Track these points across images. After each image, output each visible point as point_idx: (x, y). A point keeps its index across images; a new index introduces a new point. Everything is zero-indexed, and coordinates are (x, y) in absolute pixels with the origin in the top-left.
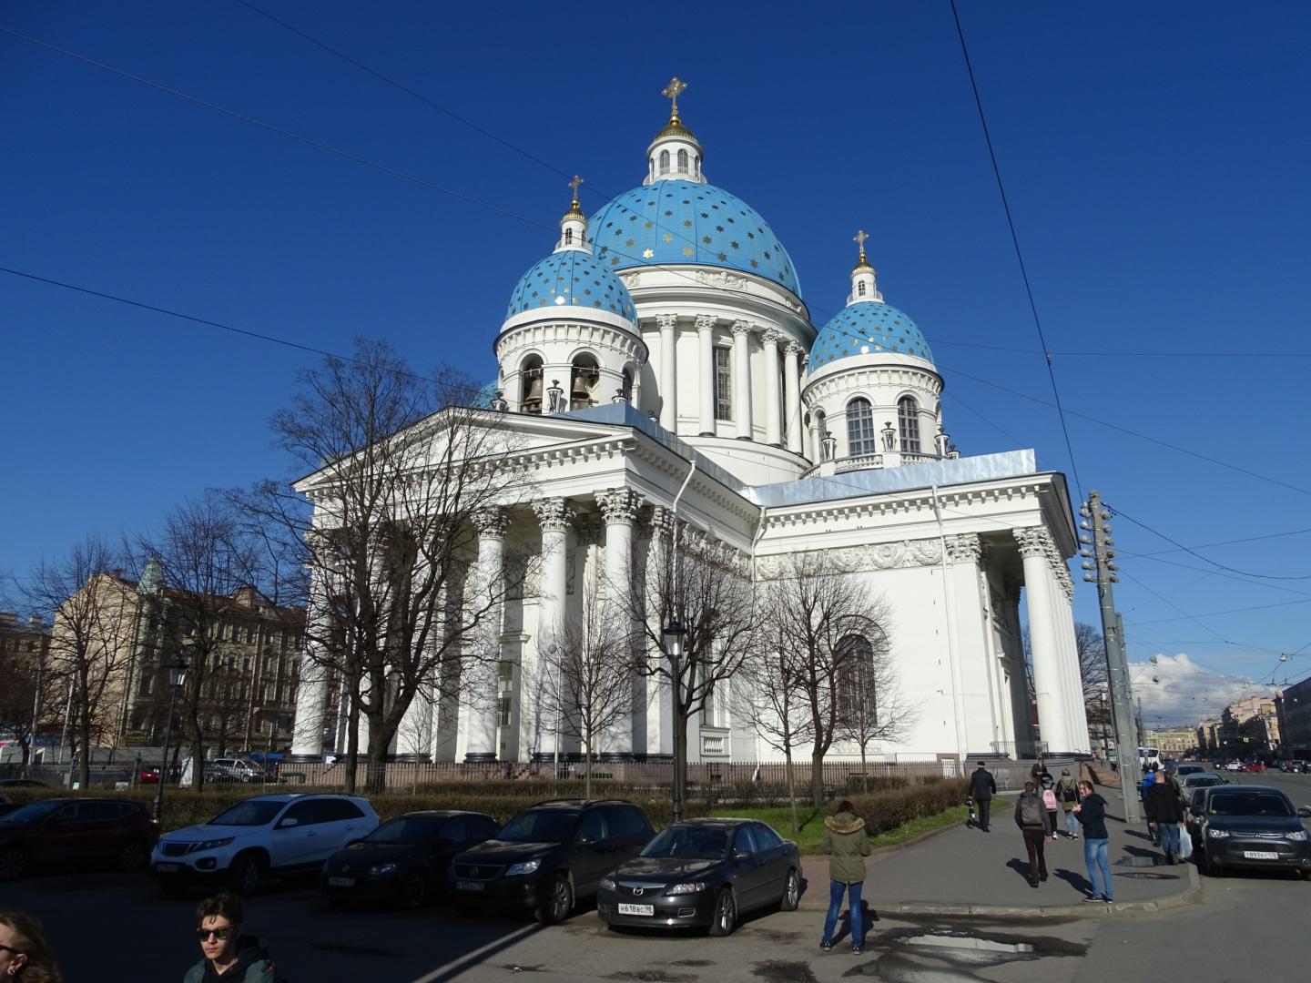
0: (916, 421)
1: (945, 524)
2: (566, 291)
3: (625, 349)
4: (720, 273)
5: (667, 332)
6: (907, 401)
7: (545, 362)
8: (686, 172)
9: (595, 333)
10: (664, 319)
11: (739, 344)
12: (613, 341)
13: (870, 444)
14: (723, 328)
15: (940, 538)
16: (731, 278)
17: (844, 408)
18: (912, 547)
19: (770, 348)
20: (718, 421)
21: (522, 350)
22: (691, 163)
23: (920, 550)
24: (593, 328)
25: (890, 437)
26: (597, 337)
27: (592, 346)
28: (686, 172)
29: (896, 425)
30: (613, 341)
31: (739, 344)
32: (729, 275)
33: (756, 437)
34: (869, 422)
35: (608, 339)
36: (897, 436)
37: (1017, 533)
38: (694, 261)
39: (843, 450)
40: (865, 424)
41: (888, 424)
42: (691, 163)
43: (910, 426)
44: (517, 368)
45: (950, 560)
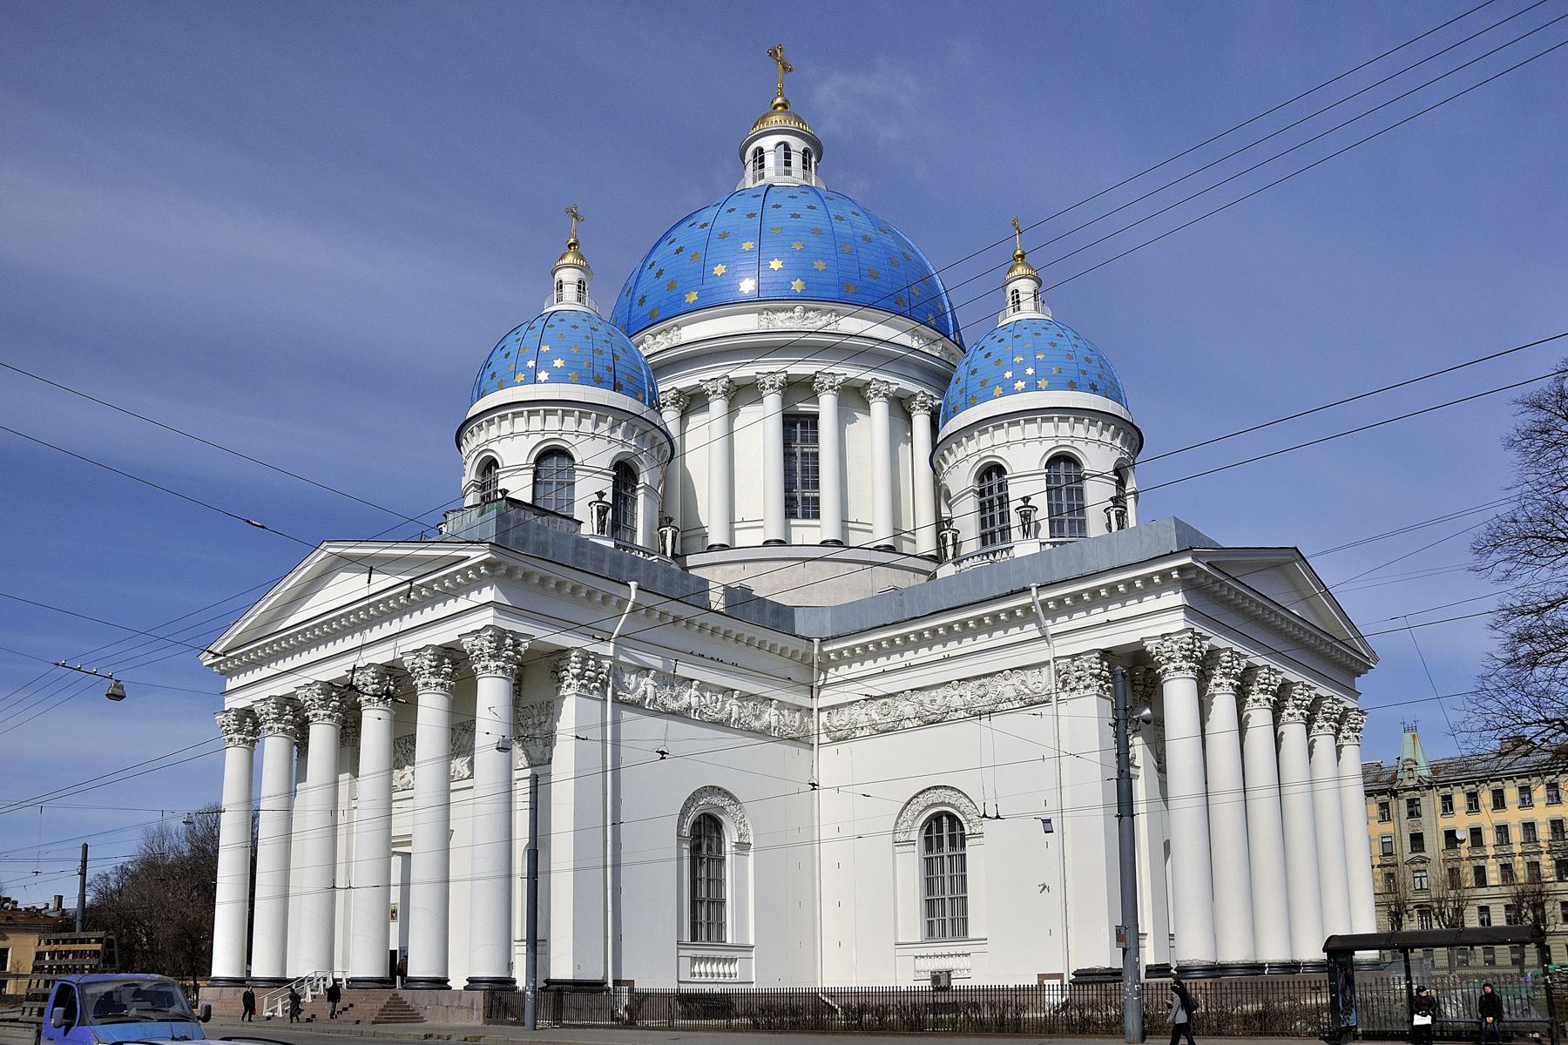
0: (1080, 491)
1: (1057, 642)
2: (531, 364)
4: (792, 310)
5: (718, 406)
6: (1062, 464)
7: (500, 466)
8: (788, 173)
10: (710, 386)
11: (826, 406)
12: (596, 426)
13: (1005, 532)
14: (797, 388)
15: (1047, 663)
16: (811, 314)
17: (970, 483)
18: (1015, 680)
19: (879, 408)
20: (793, 522)
21: (476, 453)
22: (796, 160)
23: (1023, 682)
25: (1026, 518)
26: (570, 423)
27: (563, 437)
28: (788, 173)
29: (1041, 502)
30: (596, 426)
31: (826, 406)
32: (806, 310)
33: (855, 539)
34: (1004, 501)
36: (1042, 514)
37: (1150, 646)
38: (777, 295)
39: (971, 545)
40: (1001, 505)
41: (1026, 499)
42: (796, 160)
43: (1069, 497)
45: (1063, 695)
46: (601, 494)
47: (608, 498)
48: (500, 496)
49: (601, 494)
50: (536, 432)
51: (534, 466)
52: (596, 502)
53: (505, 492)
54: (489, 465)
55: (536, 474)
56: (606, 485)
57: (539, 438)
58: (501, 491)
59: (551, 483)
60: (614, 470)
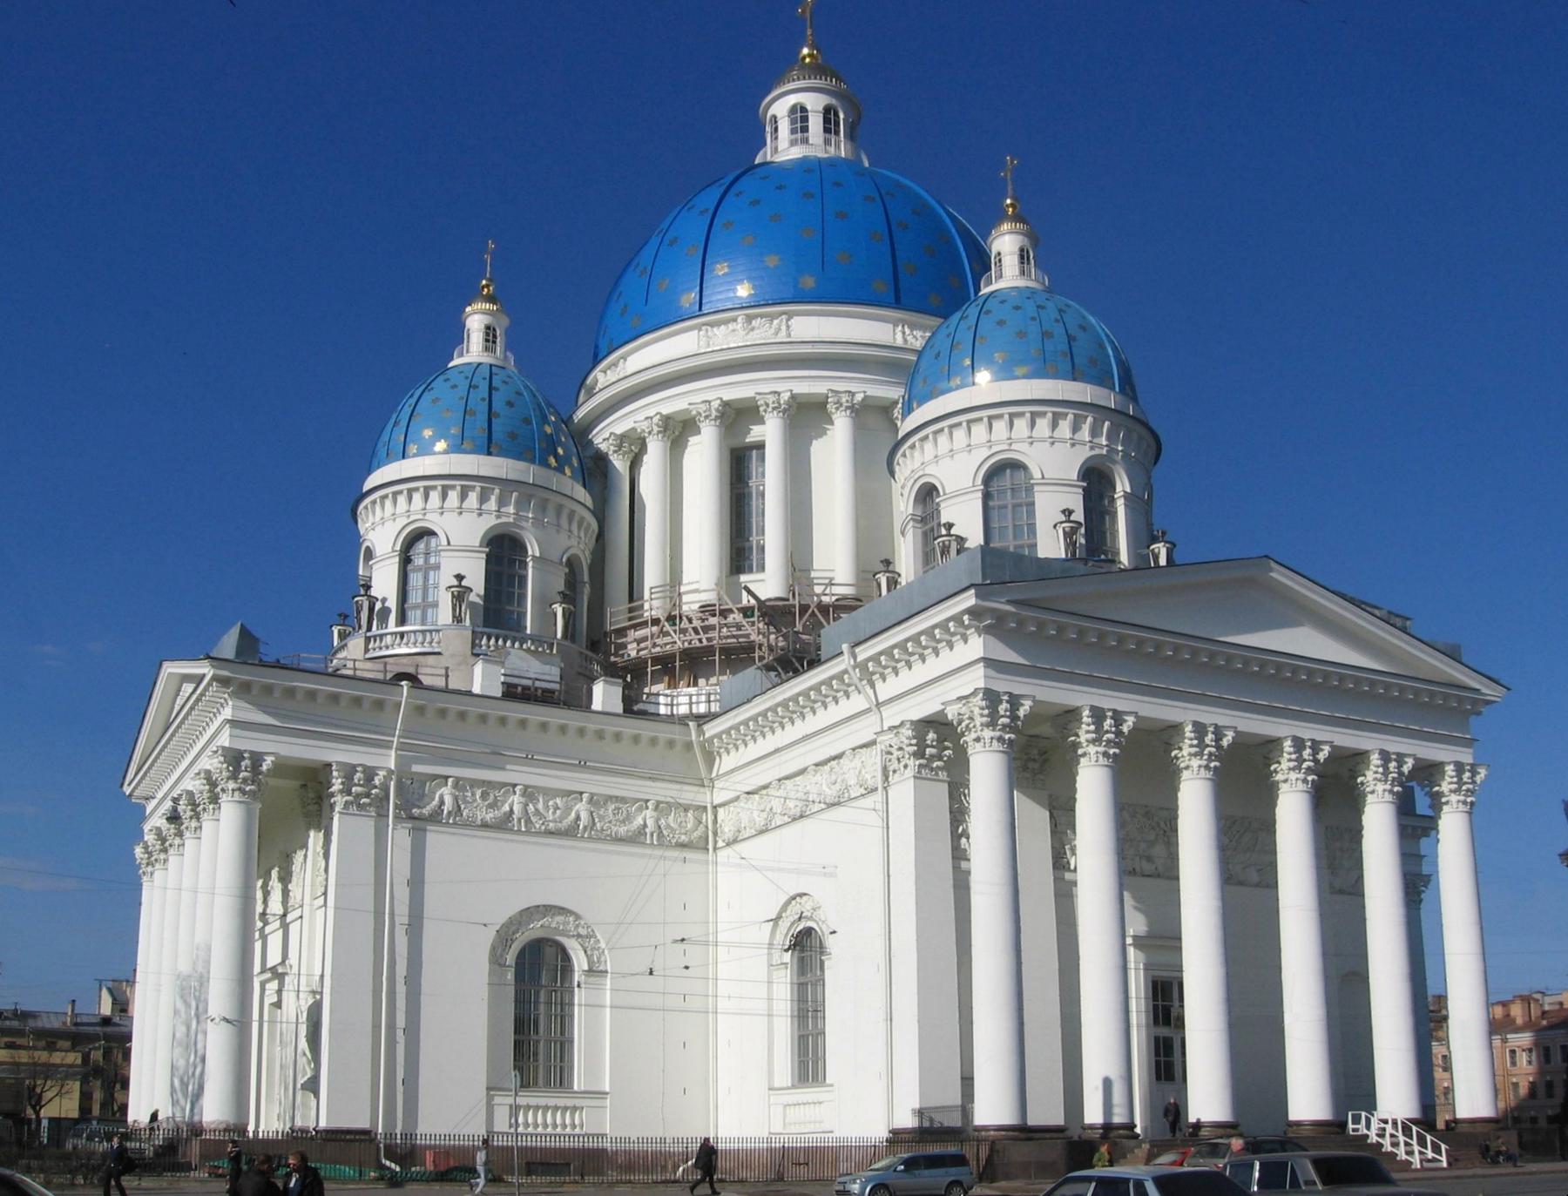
3: (1085, 434)
7: (941, 493)
9: (1016, 422)
21: (912, 481)
24: (1032, 413)
35: (1043, 425)
44: (910, 511)
46: (1068, 512)
47: (1079, 516)
48: (944, 532)
49: (1068, 512)
50: (979, 446)
51: (982, 487)
52: (1062, 523)
53: (950, 526)
54: (928, 494)
55: (987, 497)
56: (1076, 502)
57: (985, 453)
58: (944, 525)
59: (1005, 507)
60: (1083, 480)
